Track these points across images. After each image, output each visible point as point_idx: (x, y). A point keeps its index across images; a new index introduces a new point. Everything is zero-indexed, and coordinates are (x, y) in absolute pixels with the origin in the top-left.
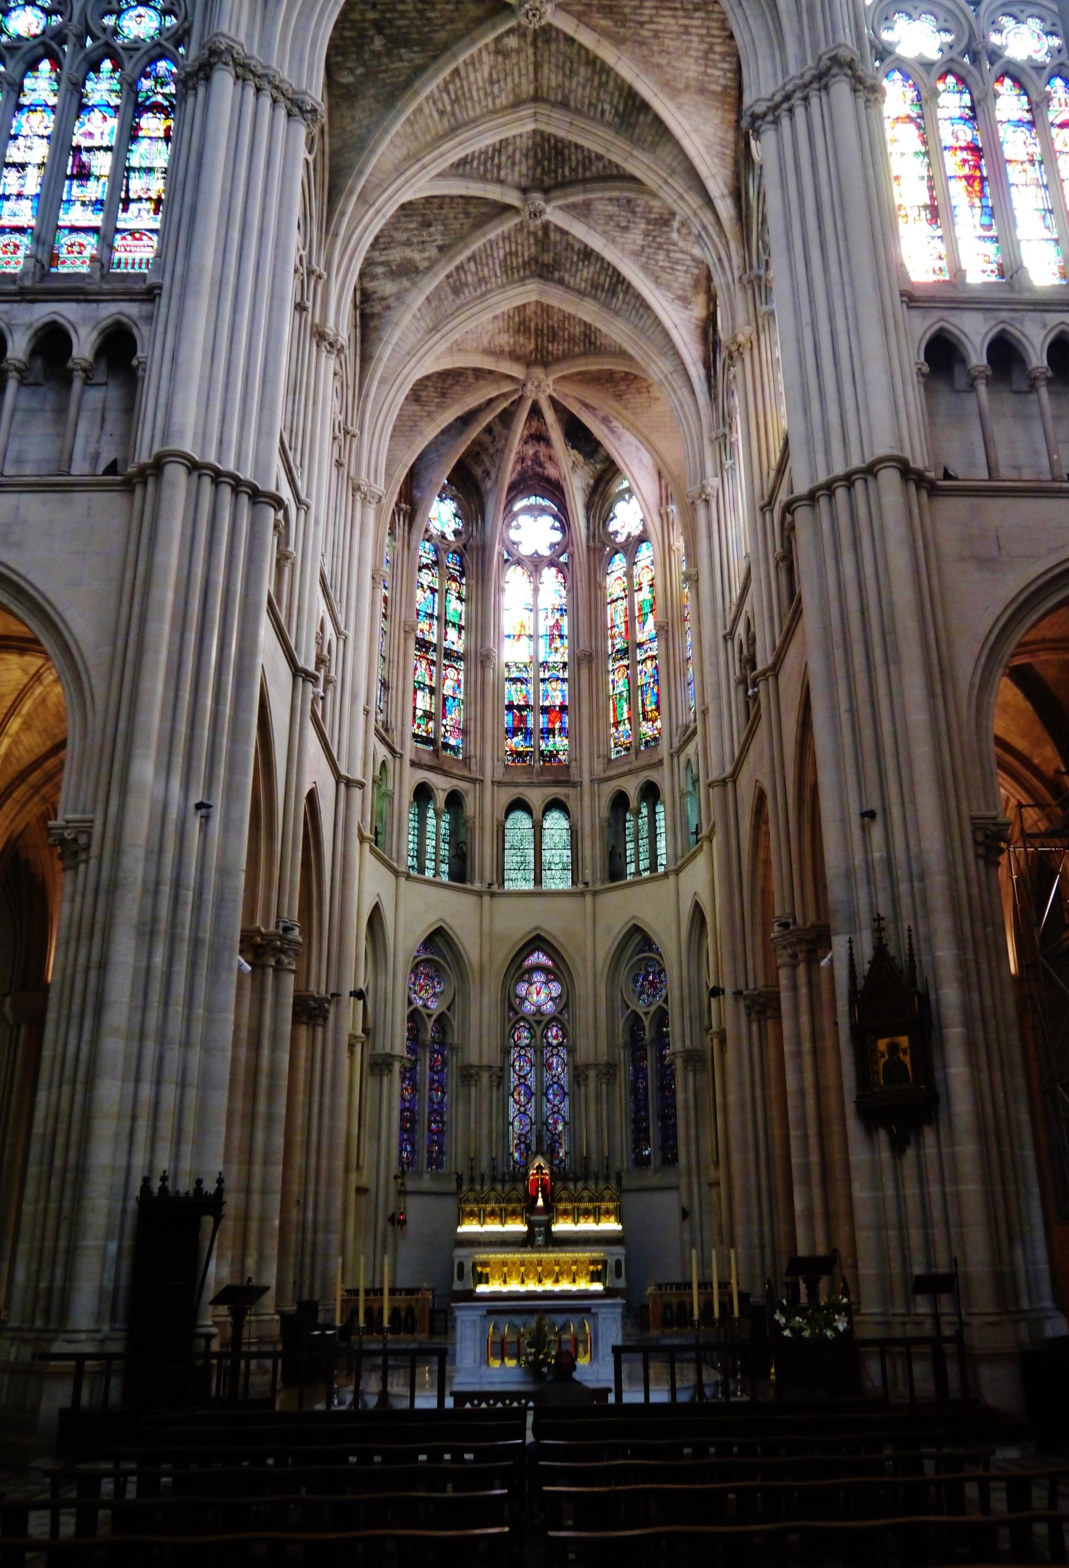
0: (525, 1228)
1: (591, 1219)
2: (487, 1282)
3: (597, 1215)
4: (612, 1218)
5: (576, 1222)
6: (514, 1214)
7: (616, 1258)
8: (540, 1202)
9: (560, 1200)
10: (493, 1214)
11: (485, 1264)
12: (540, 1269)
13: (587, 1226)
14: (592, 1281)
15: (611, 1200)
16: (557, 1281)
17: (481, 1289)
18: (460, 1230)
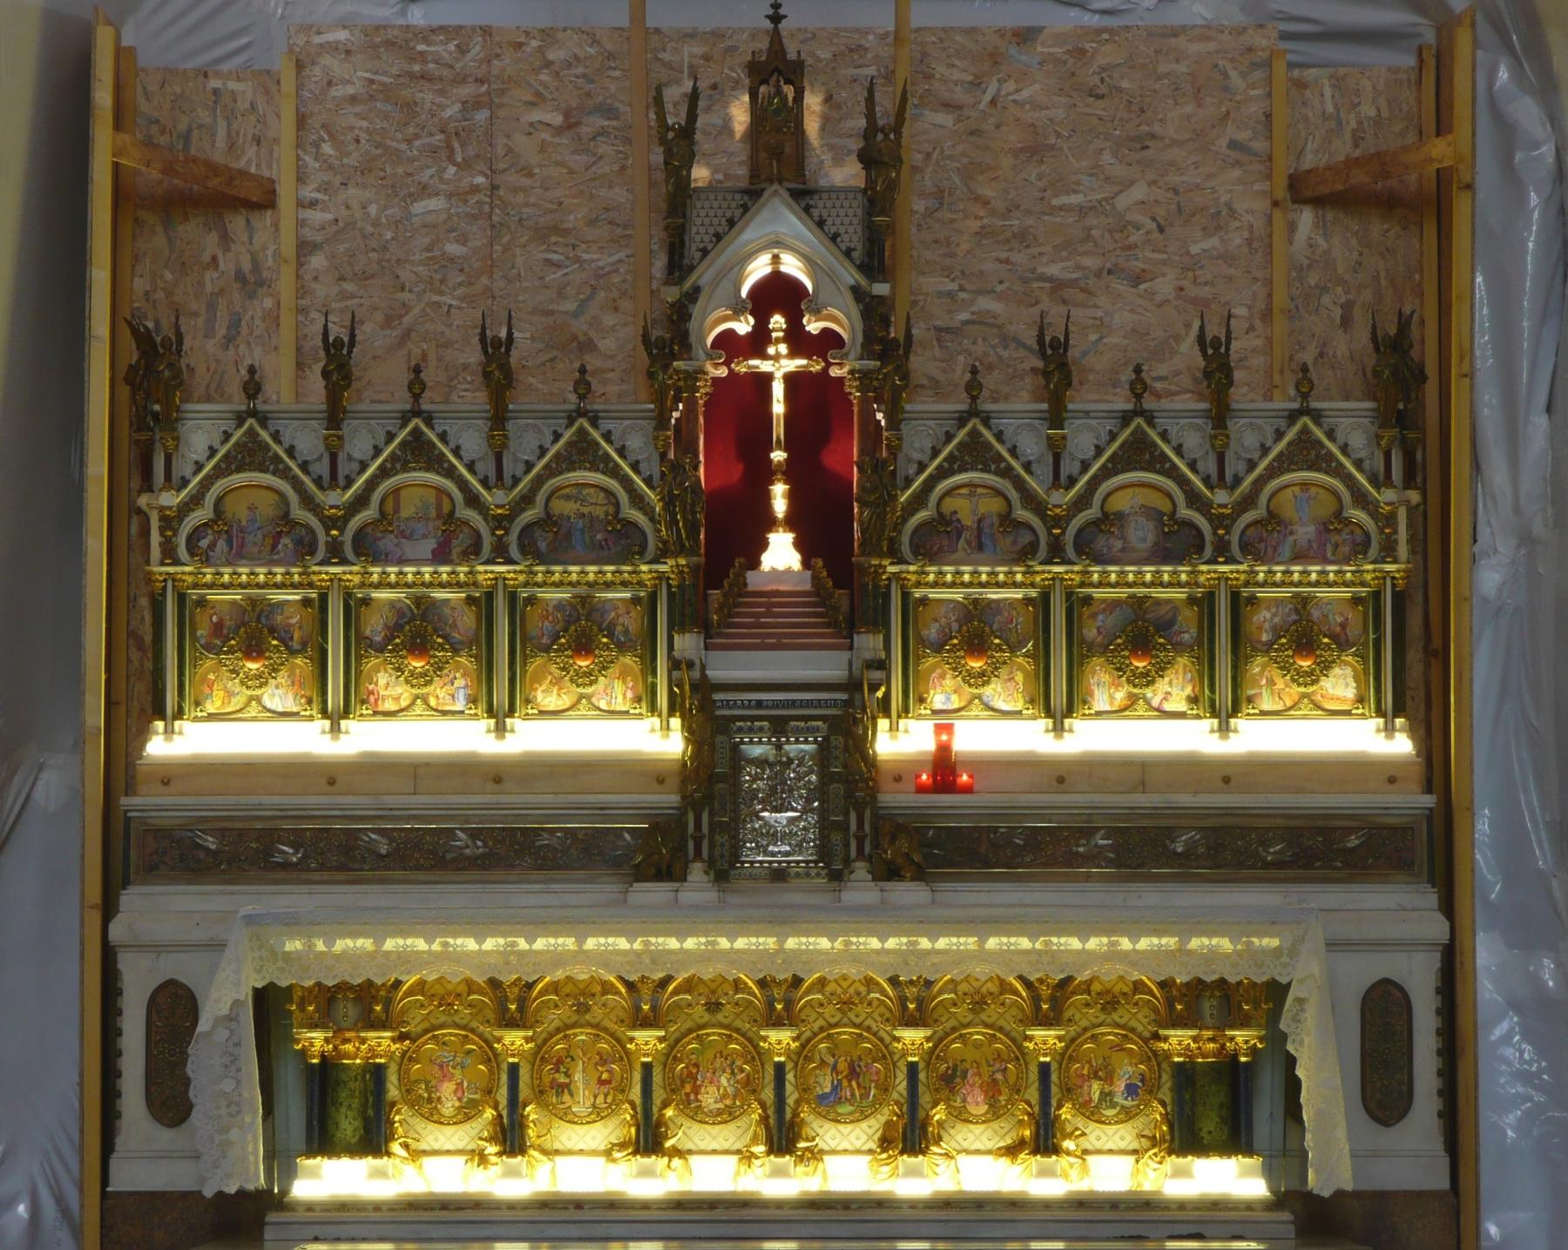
0: (661, 740)
1: (1174, 689)
2: (373, 1141)
3: (1222, 649)
4: (1340, 685)
5: (1058, 705)
6: (582, 635)
7: (1367, 970)
8: (781, 554)
9: (938, 540)
10: (417, 634)
11: (367, 1002)
12: (780, 1039)
13: (1143, 727)
14: (1185, 1138)
15: (1336, 538)
16: (910, 1136)
17: (327, 1180)
18: (159, 747)
